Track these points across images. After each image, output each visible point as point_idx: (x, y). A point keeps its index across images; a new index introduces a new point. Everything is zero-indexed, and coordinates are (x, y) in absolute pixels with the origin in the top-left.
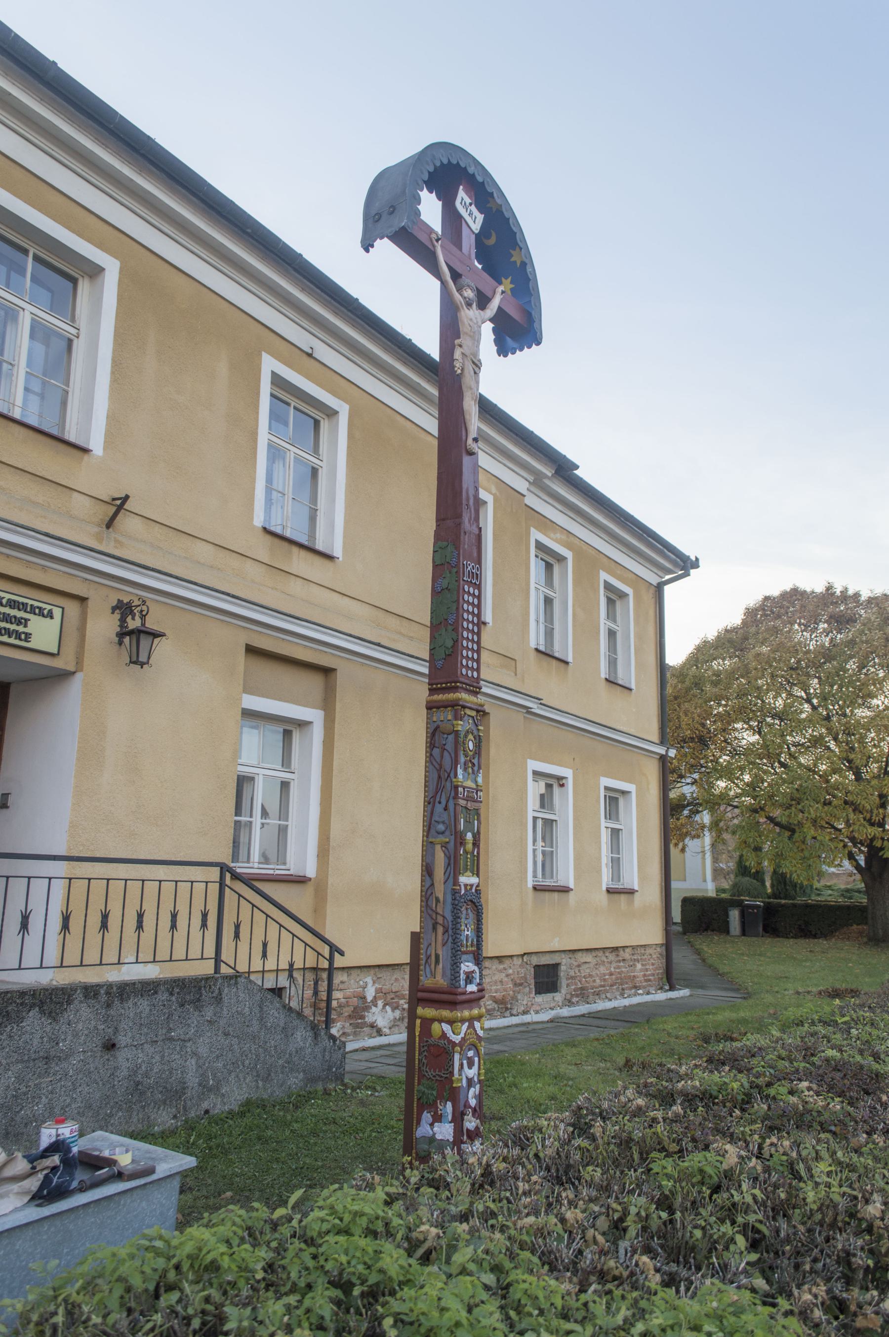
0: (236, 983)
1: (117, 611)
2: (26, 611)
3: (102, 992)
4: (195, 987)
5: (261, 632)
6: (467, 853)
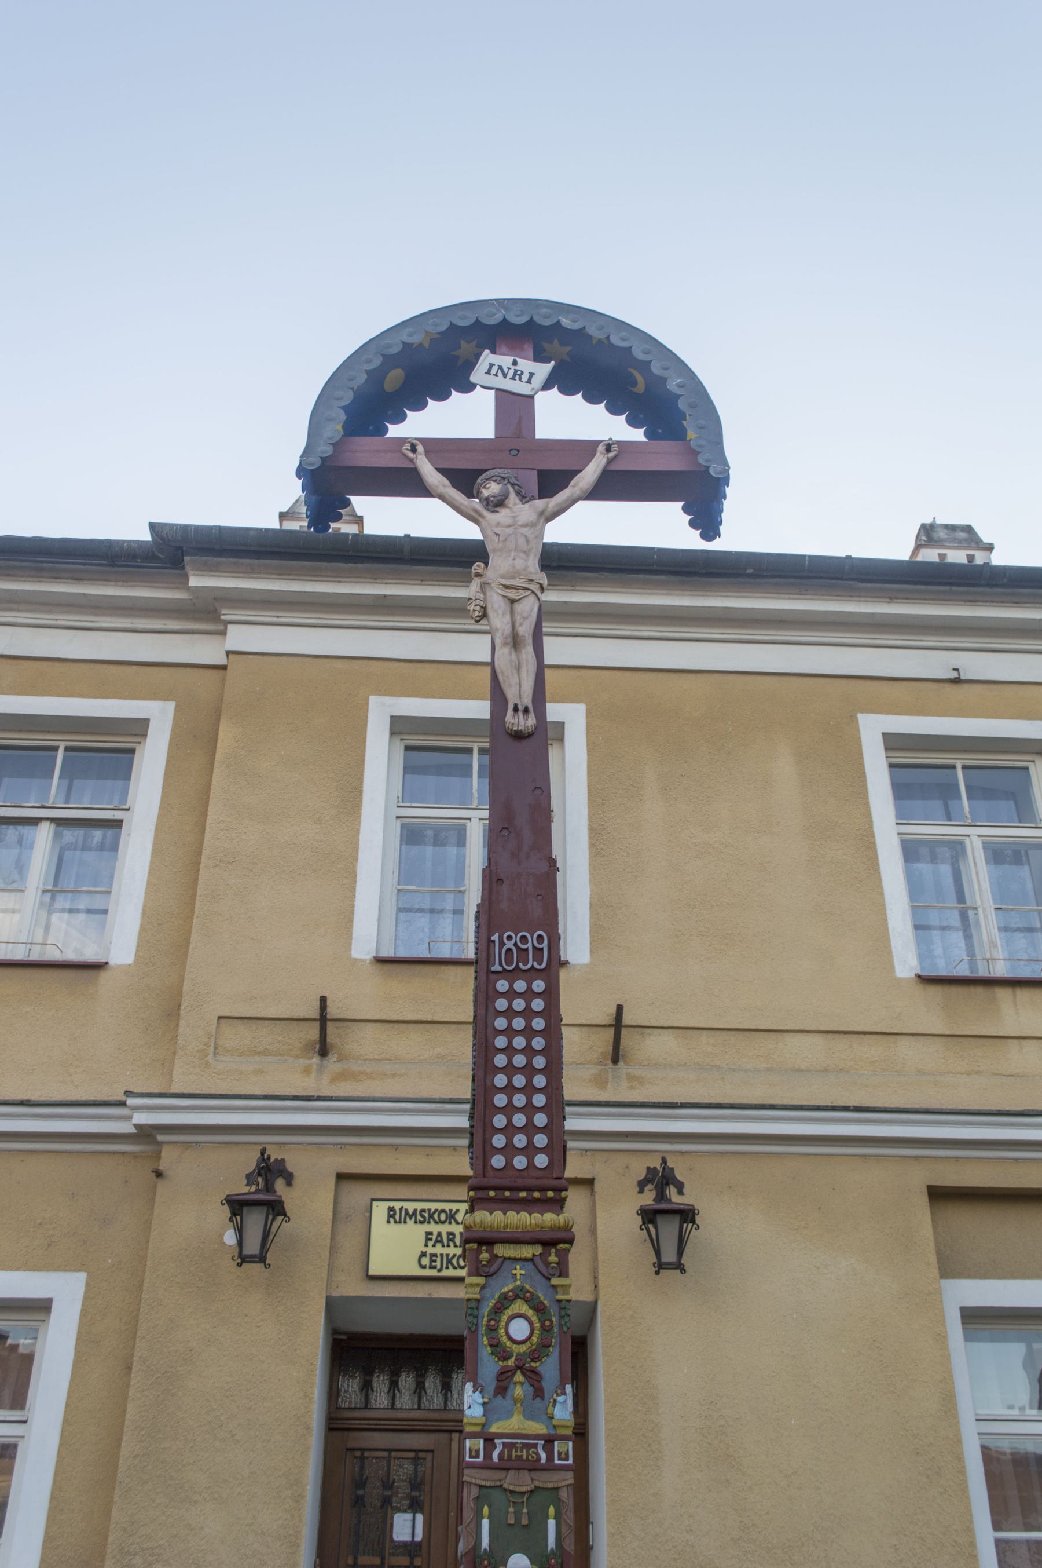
1: (650, 1186)
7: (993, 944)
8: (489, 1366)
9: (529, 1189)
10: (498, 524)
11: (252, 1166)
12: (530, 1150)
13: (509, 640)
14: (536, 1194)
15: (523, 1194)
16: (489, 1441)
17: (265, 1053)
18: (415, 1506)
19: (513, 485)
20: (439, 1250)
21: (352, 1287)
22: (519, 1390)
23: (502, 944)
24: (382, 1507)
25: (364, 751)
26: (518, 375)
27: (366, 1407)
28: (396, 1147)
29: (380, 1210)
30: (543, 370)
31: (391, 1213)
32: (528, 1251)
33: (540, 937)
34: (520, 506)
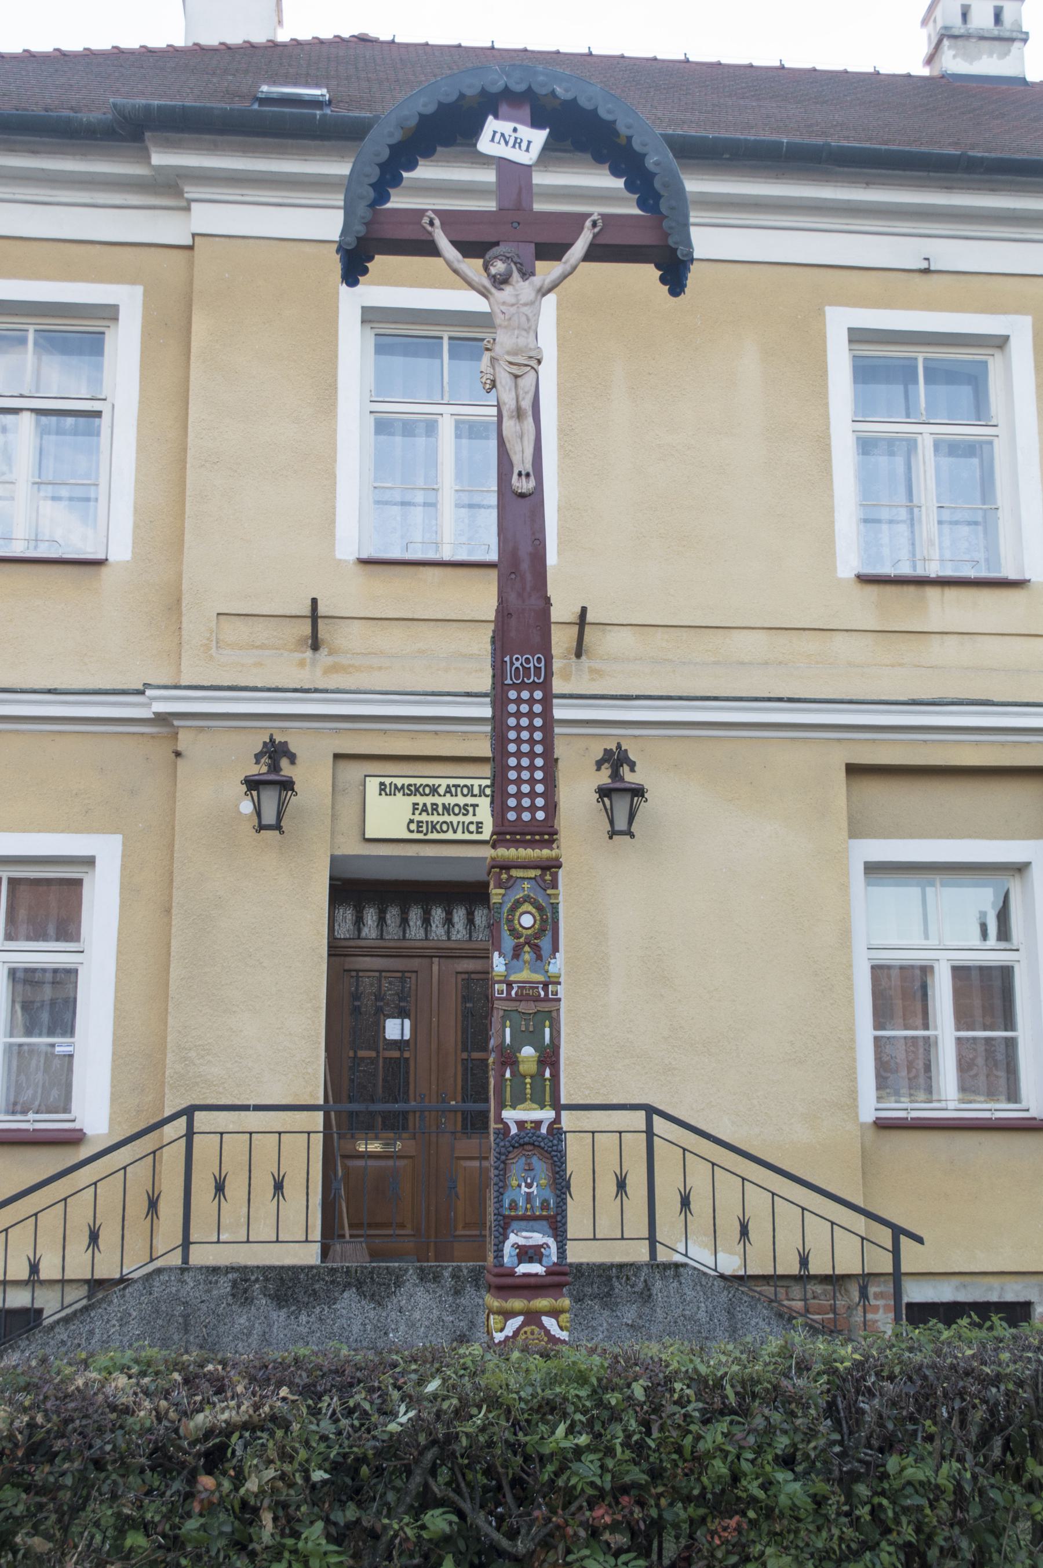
0: (677, 1275)
1: (606, 765)
2: (473, 795)
3: (446, 1274)
4: (600, 1276)
5: (874, 740)
6: (525, 1077)
7: (931, 542)
8: (508, 942)
9: (532, 834)
10: (504, 303)
11: (259, 748)
12: (533, 809)
13: (515, 413)
14: (537, 837)
15: (528, 837)
16: (510, 985)
17: (262, 647)
18: (402, 1014)
19: (515, 263)
20: (424, 817)
21: (352, 848)
22: (527, 955)
23: (512, 664)
24: (375, 1015)
25: (336, 345)
26: (517, 143)
27: (359, 938)
28: (385, 731)
29: (373, 784)
30: (539, 137)
31: (382, 787)
32: (532, 873)
33: (539, 658)
34: (522, 283)
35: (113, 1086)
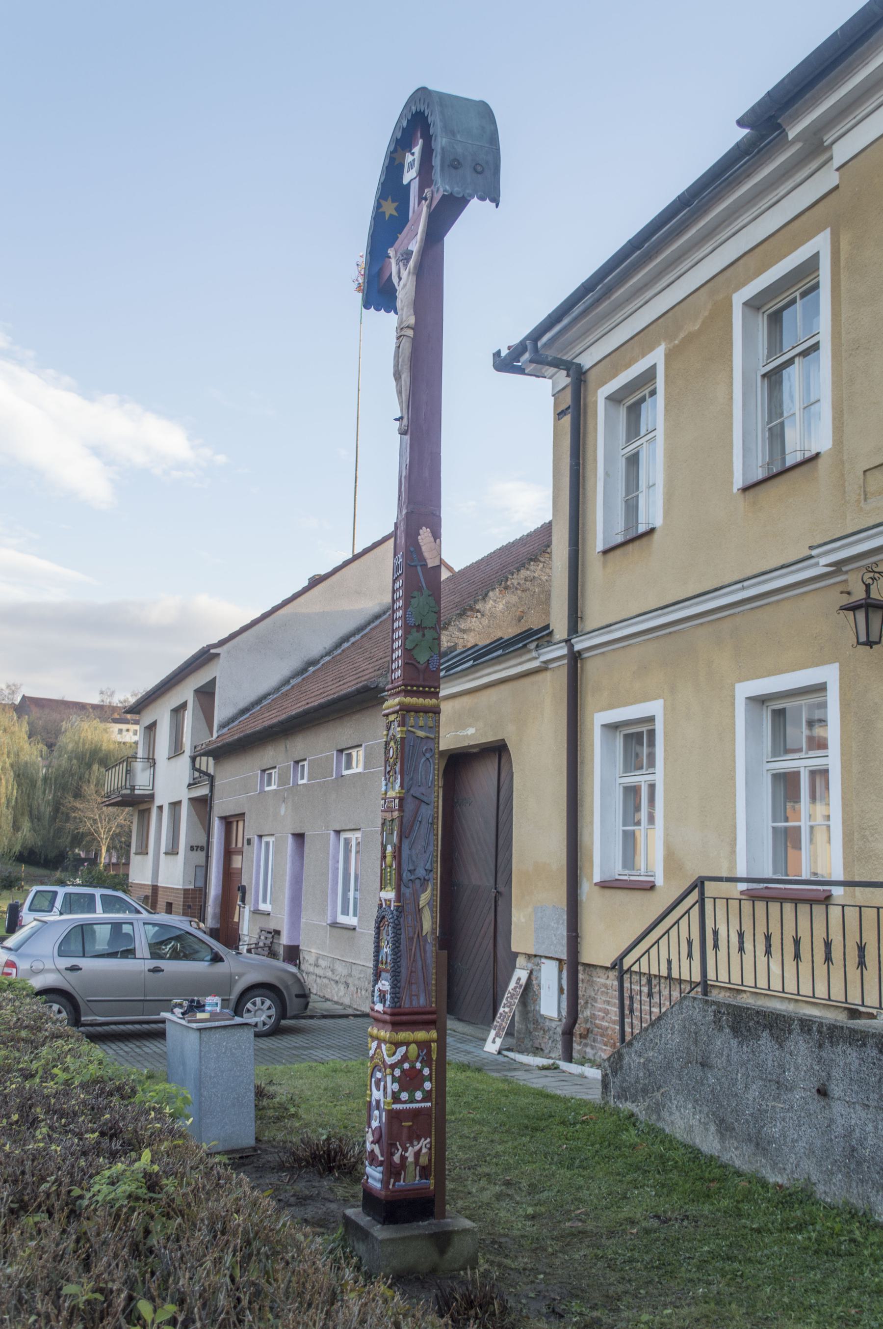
35: (844, 858)
